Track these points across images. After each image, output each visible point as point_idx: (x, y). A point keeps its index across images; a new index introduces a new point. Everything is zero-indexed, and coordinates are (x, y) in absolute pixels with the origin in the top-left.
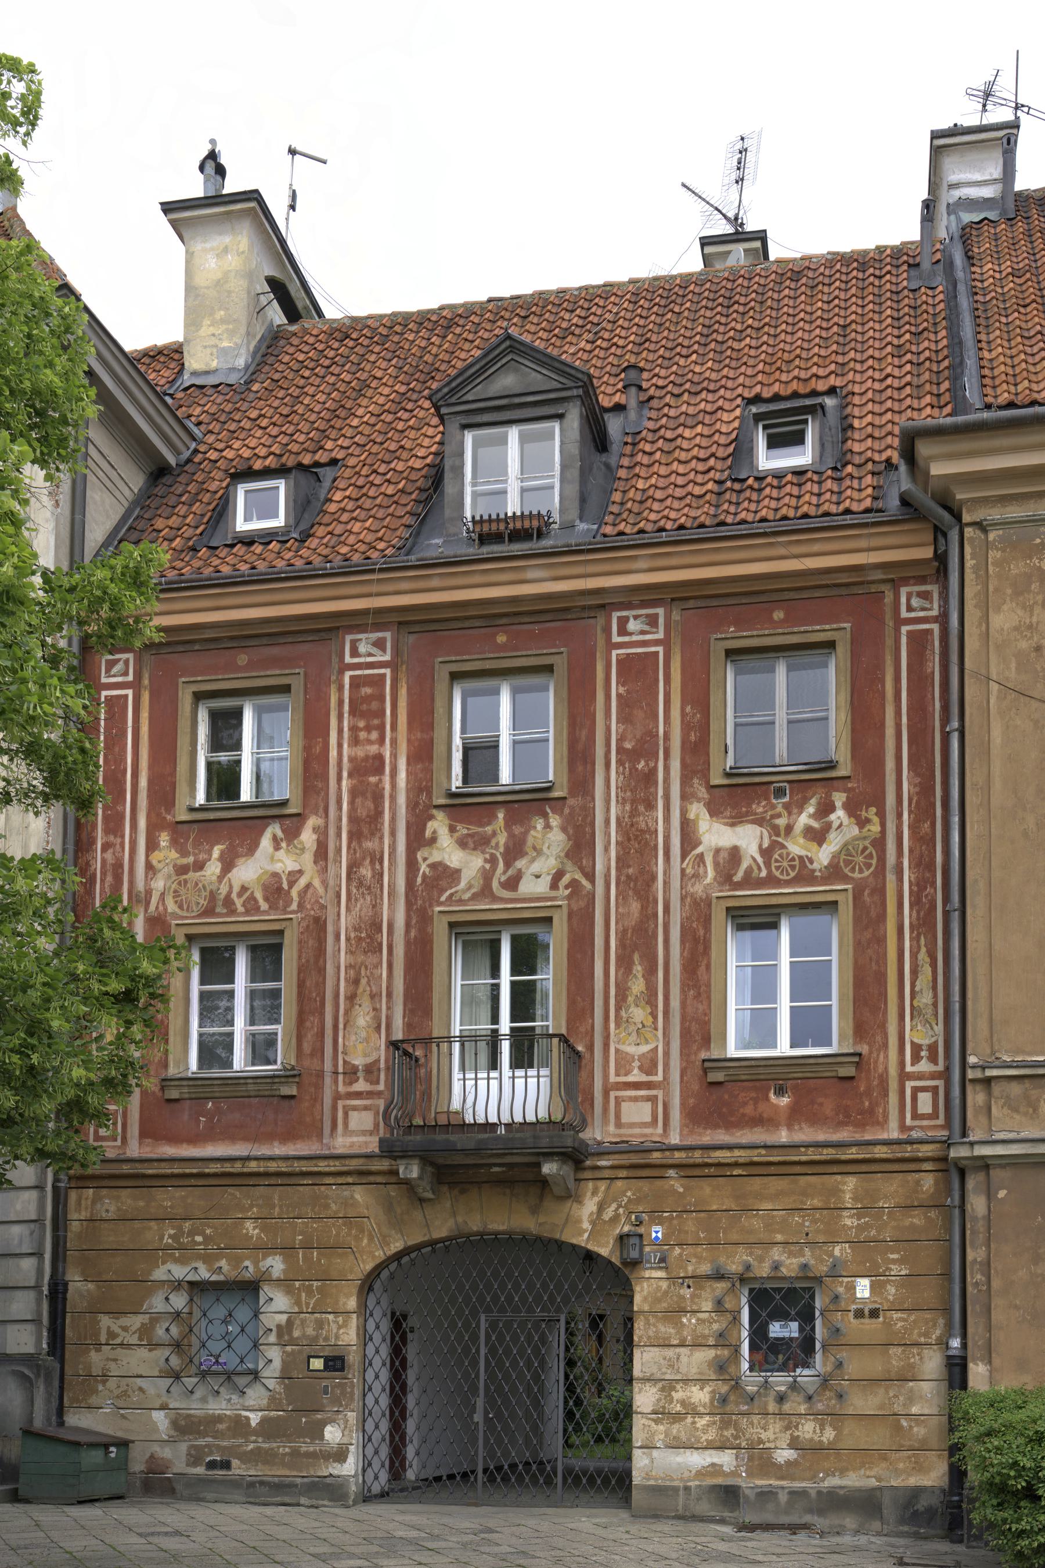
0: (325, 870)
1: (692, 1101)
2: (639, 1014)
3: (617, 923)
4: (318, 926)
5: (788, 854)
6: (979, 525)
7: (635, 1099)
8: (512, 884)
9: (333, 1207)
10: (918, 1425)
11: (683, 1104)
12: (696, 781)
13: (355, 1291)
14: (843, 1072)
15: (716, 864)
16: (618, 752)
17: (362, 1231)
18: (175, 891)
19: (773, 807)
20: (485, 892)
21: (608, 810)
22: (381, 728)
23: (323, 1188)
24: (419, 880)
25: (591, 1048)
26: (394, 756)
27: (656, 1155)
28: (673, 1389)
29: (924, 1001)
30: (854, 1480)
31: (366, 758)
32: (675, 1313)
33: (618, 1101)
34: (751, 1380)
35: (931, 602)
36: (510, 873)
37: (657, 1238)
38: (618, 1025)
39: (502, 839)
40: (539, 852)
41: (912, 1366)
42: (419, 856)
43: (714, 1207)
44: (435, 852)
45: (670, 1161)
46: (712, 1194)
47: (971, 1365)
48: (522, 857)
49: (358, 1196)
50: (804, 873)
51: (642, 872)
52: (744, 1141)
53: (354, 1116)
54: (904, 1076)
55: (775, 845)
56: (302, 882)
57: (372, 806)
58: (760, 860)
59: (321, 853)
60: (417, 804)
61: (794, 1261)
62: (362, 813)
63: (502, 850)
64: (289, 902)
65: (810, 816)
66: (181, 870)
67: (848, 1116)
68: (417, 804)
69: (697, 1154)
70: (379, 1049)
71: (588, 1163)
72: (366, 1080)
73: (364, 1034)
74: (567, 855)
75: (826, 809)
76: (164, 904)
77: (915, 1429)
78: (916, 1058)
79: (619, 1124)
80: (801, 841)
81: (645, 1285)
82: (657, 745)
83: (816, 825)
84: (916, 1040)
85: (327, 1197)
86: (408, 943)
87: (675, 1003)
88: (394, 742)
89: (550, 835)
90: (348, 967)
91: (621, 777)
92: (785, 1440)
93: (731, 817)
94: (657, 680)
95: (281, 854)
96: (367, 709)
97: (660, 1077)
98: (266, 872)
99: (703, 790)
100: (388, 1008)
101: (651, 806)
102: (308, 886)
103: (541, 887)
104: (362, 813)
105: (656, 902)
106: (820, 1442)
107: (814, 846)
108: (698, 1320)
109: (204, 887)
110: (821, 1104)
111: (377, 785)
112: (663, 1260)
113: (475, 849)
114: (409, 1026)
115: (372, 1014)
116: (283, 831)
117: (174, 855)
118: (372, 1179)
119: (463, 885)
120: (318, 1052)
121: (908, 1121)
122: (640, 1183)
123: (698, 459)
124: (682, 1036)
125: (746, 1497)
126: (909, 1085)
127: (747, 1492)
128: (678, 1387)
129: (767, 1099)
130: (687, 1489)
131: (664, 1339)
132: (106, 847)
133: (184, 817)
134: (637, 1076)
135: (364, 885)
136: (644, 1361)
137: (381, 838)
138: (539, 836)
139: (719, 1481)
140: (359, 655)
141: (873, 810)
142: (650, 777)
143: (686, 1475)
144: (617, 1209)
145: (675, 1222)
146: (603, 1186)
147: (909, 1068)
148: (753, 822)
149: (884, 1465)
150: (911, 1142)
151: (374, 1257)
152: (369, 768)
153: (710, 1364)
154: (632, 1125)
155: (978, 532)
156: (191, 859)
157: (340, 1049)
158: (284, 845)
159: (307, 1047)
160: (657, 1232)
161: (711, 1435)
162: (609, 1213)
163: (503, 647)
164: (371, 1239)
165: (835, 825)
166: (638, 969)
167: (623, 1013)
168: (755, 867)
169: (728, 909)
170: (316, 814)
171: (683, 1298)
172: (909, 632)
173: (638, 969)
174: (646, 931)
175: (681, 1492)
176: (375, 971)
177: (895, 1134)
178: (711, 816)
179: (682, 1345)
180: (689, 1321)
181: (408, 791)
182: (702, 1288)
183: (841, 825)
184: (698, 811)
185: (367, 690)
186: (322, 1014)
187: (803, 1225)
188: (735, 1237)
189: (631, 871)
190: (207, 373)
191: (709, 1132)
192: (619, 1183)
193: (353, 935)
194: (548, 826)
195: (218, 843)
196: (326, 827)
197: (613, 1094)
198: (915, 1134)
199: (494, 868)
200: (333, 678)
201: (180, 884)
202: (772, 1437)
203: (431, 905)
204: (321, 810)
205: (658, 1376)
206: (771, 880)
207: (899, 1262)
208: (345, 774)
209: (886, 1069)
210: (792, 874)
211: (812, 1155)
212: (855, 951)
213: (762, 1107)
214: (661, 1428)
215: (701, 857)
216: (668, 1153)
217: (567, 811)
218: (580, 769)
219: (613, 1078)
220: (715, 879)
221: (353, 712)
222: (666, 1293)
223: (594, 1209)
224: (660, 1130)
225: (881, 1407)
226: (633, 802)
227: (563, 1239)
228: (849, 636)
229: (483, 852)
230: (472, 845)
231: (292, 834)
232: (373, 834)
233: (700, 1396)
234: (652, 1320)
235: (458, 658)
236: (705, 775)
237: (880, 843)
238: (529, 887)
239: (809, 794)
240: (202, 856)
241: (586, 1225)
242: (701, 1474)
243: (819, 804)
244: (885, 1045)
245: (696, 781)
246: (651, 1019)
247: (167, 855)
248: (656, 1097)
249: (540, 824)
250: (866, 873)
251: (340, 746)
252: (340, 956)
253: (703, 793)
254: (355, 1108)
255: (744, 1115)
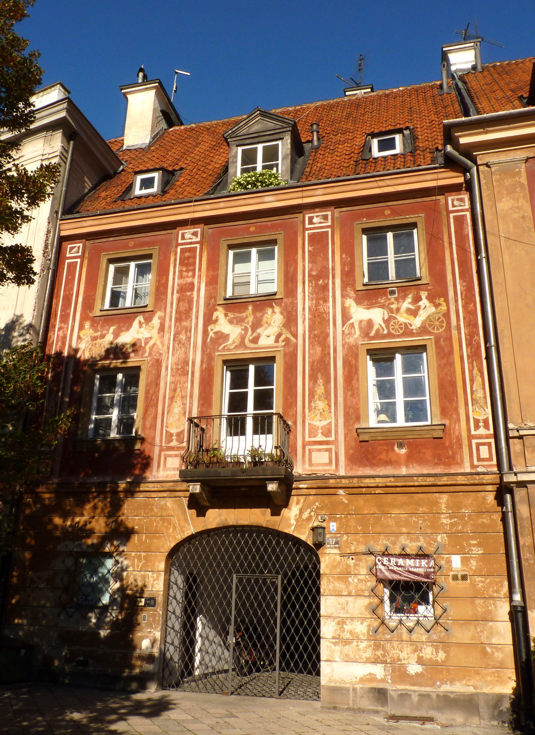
0: (163, 336)
1: (351, 451)
2: (321, 405)
3: (309, 358)
4: (158, 363)
5: (398, 322)
6: (487, 165)
7: (320, 450)
8: (255, 340)
9: (155, 510)
10: (497, 651)
11: (346, 453)
12: (348, 289)
13: (164, 559)
14: (436, 435)
15: (360, 328)
16: (309, 276)
17: (170, 524)
18: (90, 349)
19: (389, 299)
20: (242, 344)
21: (304, 303)
22: (194, 271)
23: (150, 499)
24: (209, 340)
25: (295, 423)
26: (199, 283)
27: (332, 481)
28: (344, 623)
29: (479, 395)
30: (459, 688)
31: (186, 284)
32: (345, 575)
33: (310, 451)
34: (393, 619)
35: (464, 202)
36: (254, 335)
37: (333, 530)
38: (310, 410)
39: (251, 319)
40: (269, 324)
41: (490, 612)
42: (209, 328)
43: (366, 512)
44: (217, 326)
45: (340, 486)
46: (365, 505)
47: (529, 612)
48: (260, 327)
49: (168, 504)
50: (407, 331)
51: (322, 333)
52: (381, 474)
53: (169, 460)
54: (470, 437)
55: (391, 318)
56: (151, 343)
57: (187, 306)
58: (383, 325)
59: (162, 329)
60: (209, 304)
61: (414, 544)
62: (182, 309)
63: (250, 324)
64: (144, 353)
65: (409, 303)
66: (94, 339)
67: (440, 459)
68: (209, 304)
69: (355, 480)
70: (184, 424)
71: (294, 486)
72: (177, 441)
73: (177, 417)
74: (283, 326)
75: (417, 299)
76: (84, 355)
77: (496, 654)
78: (477, 427)
79: (311, 464)
80: (405, 315)
81: (327, 557)
82: (329, 272)
83: (412, 307)
84: (476, 417)
85: (152, 505)
86: (202, 371)
87: (340, 399)
88: (200, 276)
89: (274, 316)
90: (171, 383)
91: (311, 288)
92: (414, 658)
93: (367, 305)
94: (328, 243)
95: (142, 330)
96: (188, 261)
97: (333, 438)
98: (134, 338)
99: (353, 293)
100: (190, 403)
101: (326, 300)
102: (154, 344)
103: (271, 341)
104: (182, 309)
105: (329, 347)
106: (436, 660)
107: (412, 317)
108: (358, 580)
109: (104, 346)
110: (424, 453)
111: (190, 296)
112: (337, 543)
113: (237, 324)
114: (200, 412)
115: (182, 406)
116: (144, 319)
117: (91, 331)
118: (177, 494)
119: (230, 342)
120: (153, 426)
121: (476, 462)
122: (323, 497)
123: (346, 154)
124: (345, 416)
125: (391, 696)
126: (474, 442)
127: (392, 693)
128: (348, 622)
129: (393, 450)
130: (354, 689)
131: (339, 591)
132: (59, 330)
133: (98, 313)
134: (320, 438)
135: (181, 341)
136: (327, 605)
137: (191, 320)
138: (269, 317)
139: (375, 685)
140: (185, 239)
141: (442, 299)
142: (325, 288)
143: (354, 680)
144: (310, 513)
145: (344, 520)
146: (302, 499)
147: (473, 432)
148: (379, 307)
149: (478, 678)
150: (478, 474)
151: (175, 539)
152: (186, 289)
153: (367, 608)
154: (318, 465)
155: (487, 168)
156: (99, 333)
157: (165, 425)
158: (144, 325)
159: (148, 424)
160: (333, 526)
161: (369, 654)
162: (305, 515)
163: (253, 233)
164: (174, 528)
165: (422, 307)
166: (320, 381)
167: (312, 404)
168: (381, 329)
169: (368, 350)
170: (161, 311)
171: (349, 566)
172: (453, 216)
173: (320, 381)
174: (324, 362)
175: (351, 692)
176: (184, 385)
177: (468, 470)
178: (357, 305)
179: (349, 595)
180: (353, 580)
181: (205, 298)
182: (360, 560)
183: (425, 307)
184: (350, 302)
185: (187, 254)
186: (156, 406)
187: (418, 523)
188: (378, 529)
189: (316, 332)
190: (133, 146)
191: (361, 468)
192: (311, 498)
193: (174, 367)
194: (274, 312)
195: (113, 326)
196: (165, 316)
197: (307, 448)
198: (479, 470)
199: (246, 333)
200: (173, 250)
201: (92, 345)
202: (406, 657)
203: (214, 352)
204: (163, 309)
205: (335, 615)
206: (390, 335)
207: (478, 545)
208: (175, 291)
209: (460, 433)
210: (401, 332)
211: (420, 481)
212: (438, 370)
213: (391, 454)
214: (338, 648)
215: (352, 325)
216: (338, 480)
217: (283, 305)
218: (290, 285)
219: (307, 439)
220: (360, 335)
221: (180, 264)
222: (339, 563)
223: (297, 512)
224: (334, 467)
225: (473, 638)
226: (317, 299)
227: (280, 529)
228: (423, 219)
229: (241, 326)
230: (236, 323)
231: (148, 320)
232: (187, 319)
233: (361, 628)
234: (331, 580)
235: (232, 238)
236: (353, 285)
237: (447, 315)
238: (263, 342)
239: (408, 292)
240: (104, 332)
241: (293, 522)
242: (362, 680)
243: (413, 297)
244: (458, 420)
245: (348, 289)
246: (327, 407)
247: (88, 331)
248: (331, 449)
249: (270, 311)
250: (441, 330)
251: (174, 279)
252: (167, 377)
253: (352, 294)
254: (170, 456)
255: (380, 459)
